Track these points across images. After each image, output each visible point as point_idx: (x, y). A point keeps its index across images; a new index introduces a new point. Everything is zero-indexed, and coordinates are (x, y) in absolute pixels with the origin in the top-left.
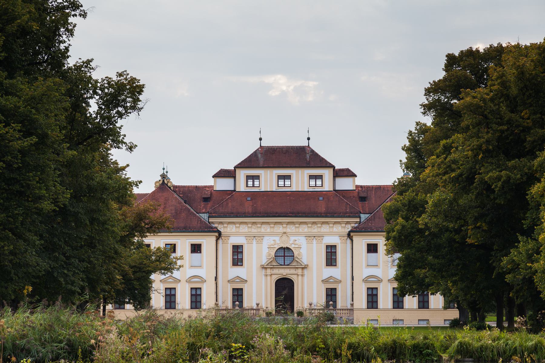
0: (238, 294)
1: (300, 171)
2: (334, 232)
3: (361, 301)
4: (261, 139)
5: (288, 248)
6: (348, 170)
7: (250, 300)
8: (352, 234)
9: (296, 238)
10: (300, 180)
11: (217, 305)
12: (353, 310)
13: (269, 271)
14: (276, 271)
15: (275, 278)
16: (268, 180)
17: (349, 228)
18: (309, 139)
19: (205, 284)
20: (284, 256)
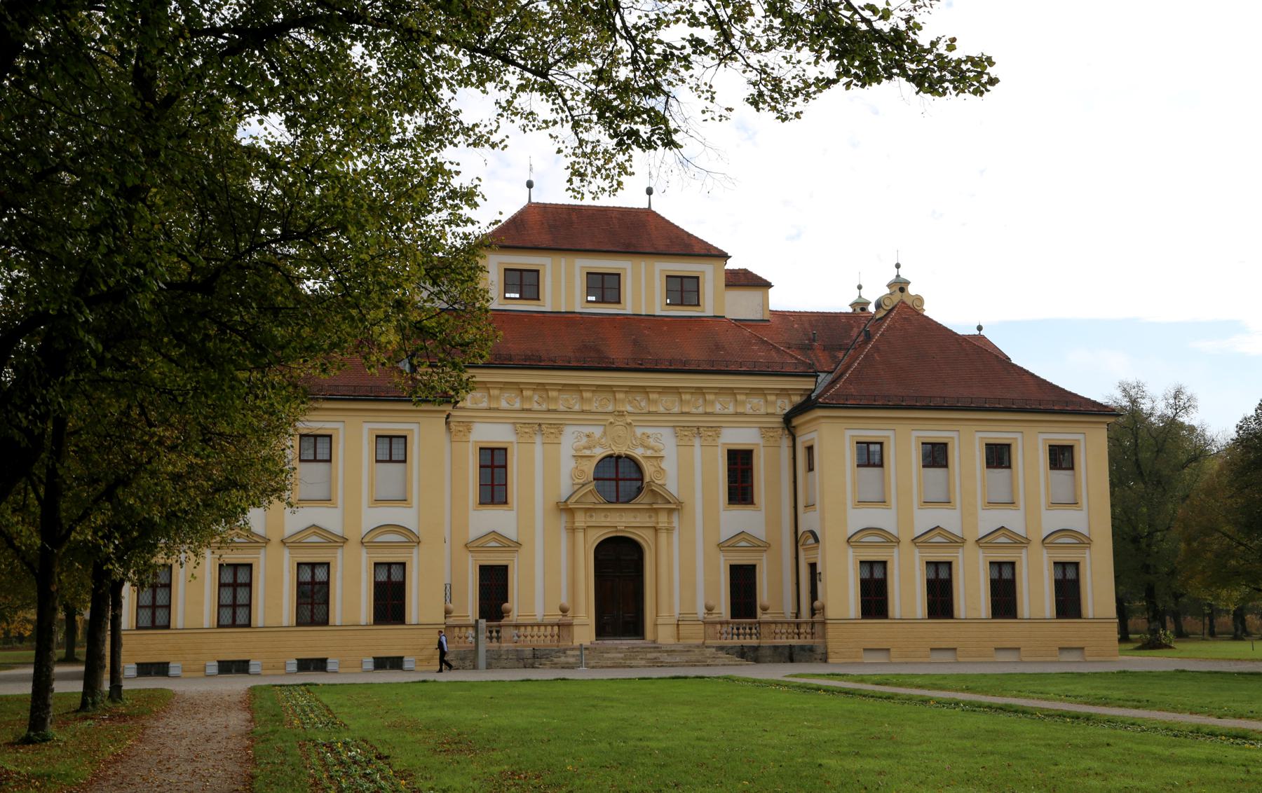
0: (494, 585)
1: (643, 264)
2: (745, 416)
3: (843, 596)
4: (530, 185)
5: (629, 457)
6: (745, 273)
7: (530, 599)
9: (649, 431)
10: (644, 288)
11: (448, 613)
12: (824, 623)
13: (580, 520)
14: (599, 519)
15: (596, 537)
16: (564, 285)
17: (784, 406)
18: (649, 191)
19: (415, 551)
20: (617, 480)
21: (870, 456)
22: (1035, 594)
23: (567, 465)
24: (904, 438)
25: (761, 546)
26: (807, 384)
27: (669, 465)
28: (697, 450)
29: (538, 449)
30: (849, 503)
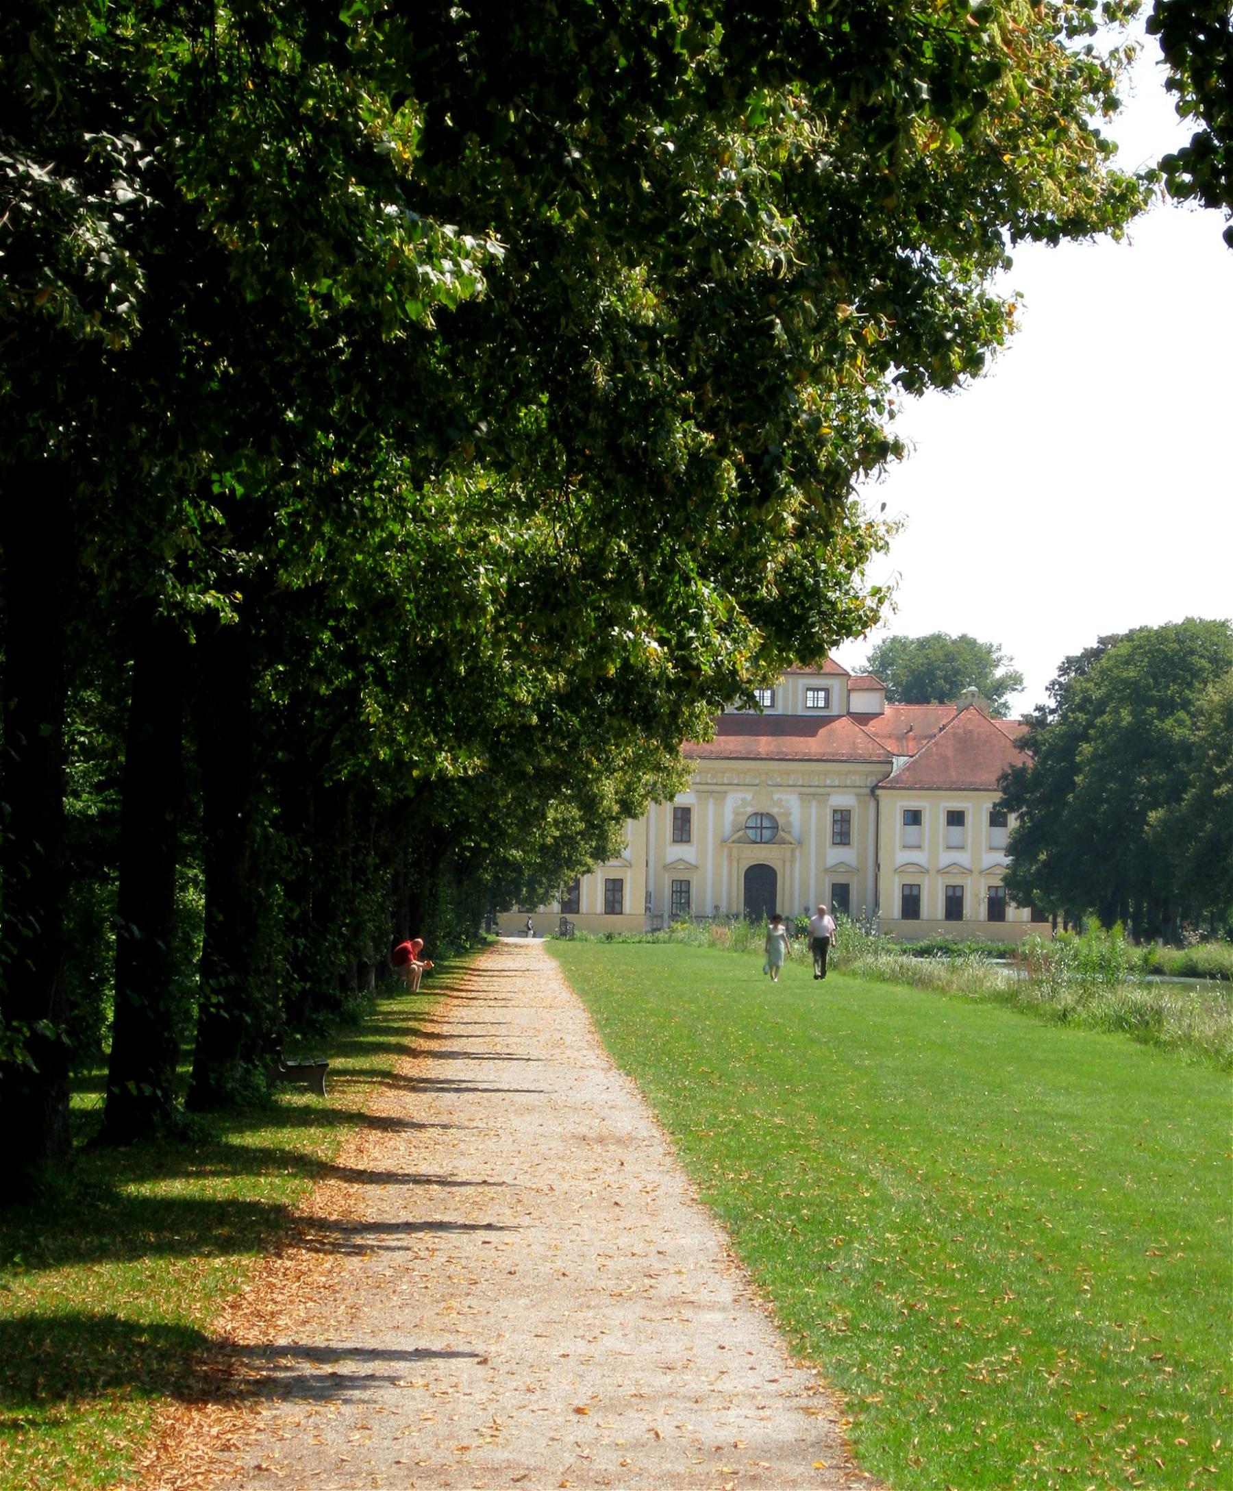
3: (892, 904)
8: (879, 792)
9: (784, 797)
11: (647, 909)
15: (745, 865)
17: (872, 781)
21: (914, 818)
22: (975, 907)
23: (729, 817)
24: (934, 808)
25: (852, 871)
26: (886, 768)
27: (796, 818)
28: (814, 810)
29: (711, 808)
30: (898, 846)
